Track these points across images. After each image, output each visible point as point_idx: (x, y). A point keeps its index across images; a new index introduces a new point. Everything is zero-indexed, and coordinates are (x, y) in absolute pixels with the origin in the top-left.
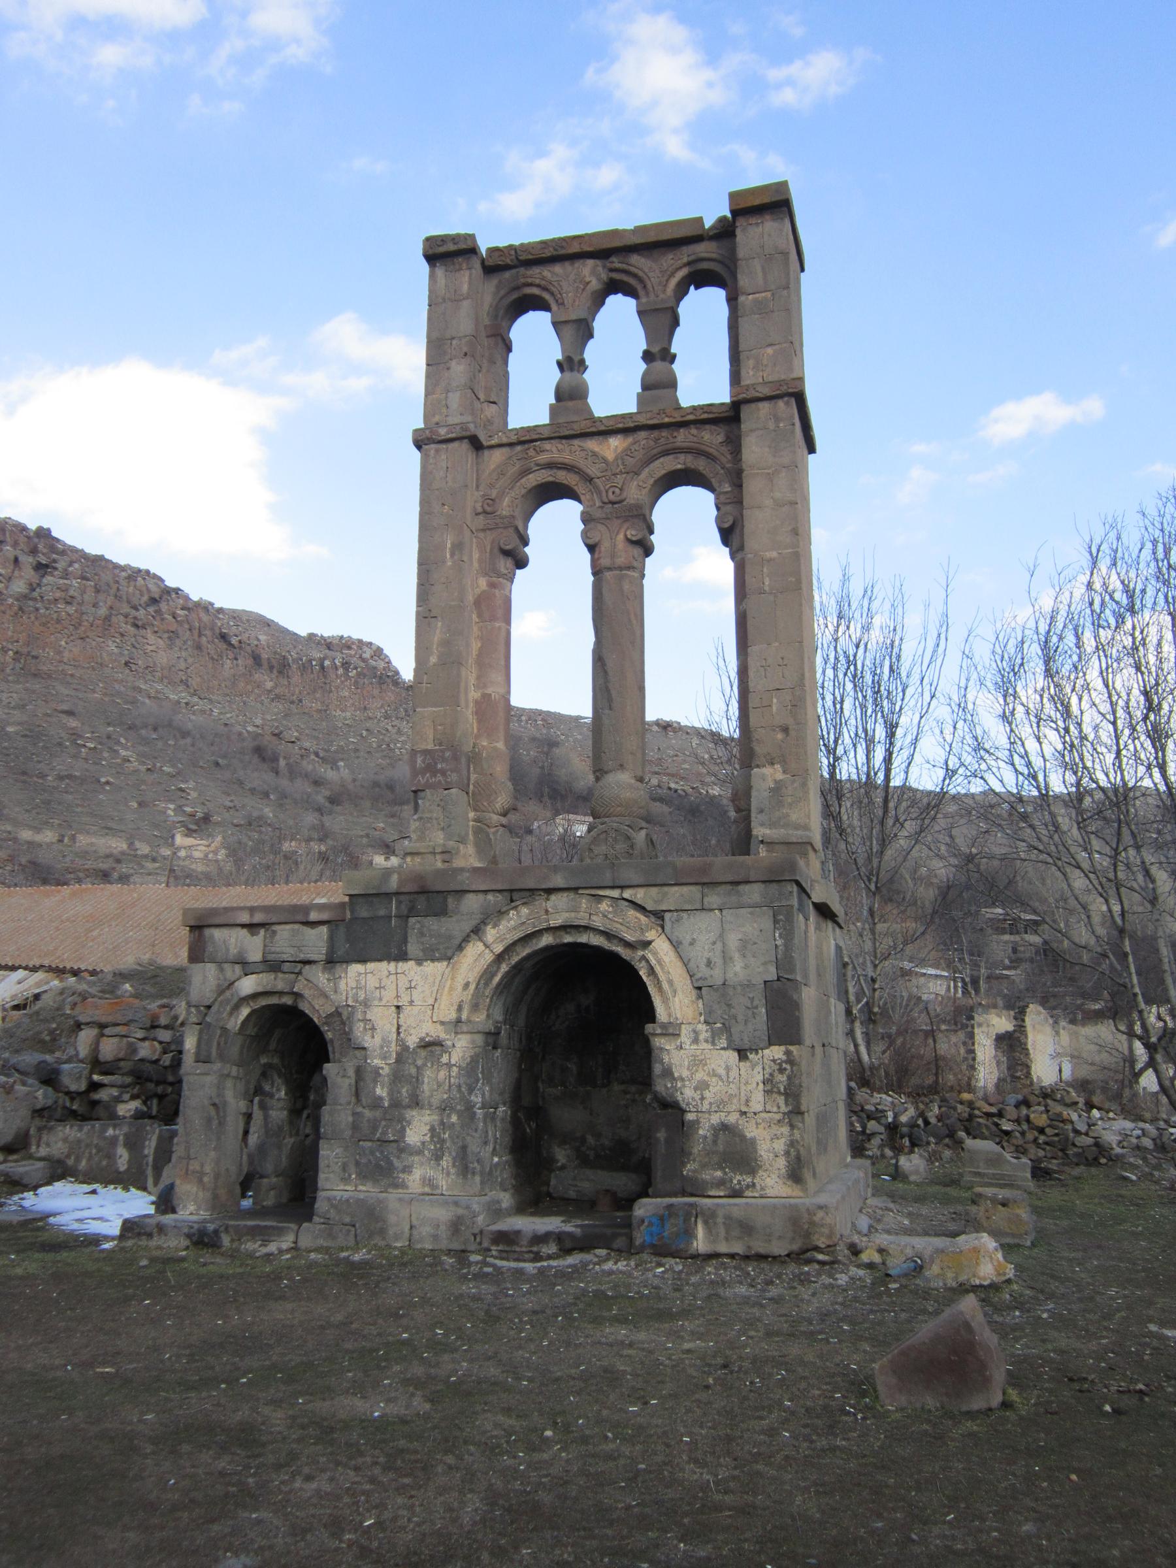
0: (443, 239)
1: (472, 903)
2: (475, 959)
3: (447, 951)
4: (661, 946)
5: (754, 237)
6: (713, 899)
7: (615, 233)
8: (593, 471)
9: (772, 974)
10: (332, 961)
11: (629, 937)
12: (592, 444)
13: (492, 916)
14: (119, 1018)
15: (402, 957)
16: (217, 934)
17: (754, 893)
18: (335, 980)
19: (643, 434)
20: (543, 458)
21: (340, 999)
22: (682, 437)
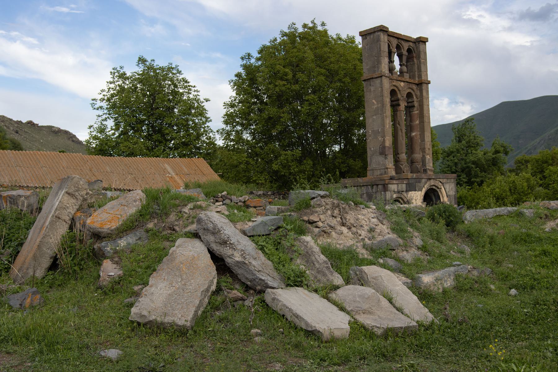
0: (384, 27)
1: (423, 181)
2: (424, 190)
3: (421, 190)
4: (443, 189)
5: (421, 46)
6: (449, 181)
7: (401, 35)
8: (401, 89)
9: (454, 193)
10: (407, 191)
11: (440, 187)
12: (399, 82)
13: (426, 183)
14: (261, 205)
15: (415, 190)
16: (390, 186)
17: (452, 180)
18: (407, 195)
19: (406, 83)
20: (394, 84)
21: (408, 198)
22: (411, 86)
